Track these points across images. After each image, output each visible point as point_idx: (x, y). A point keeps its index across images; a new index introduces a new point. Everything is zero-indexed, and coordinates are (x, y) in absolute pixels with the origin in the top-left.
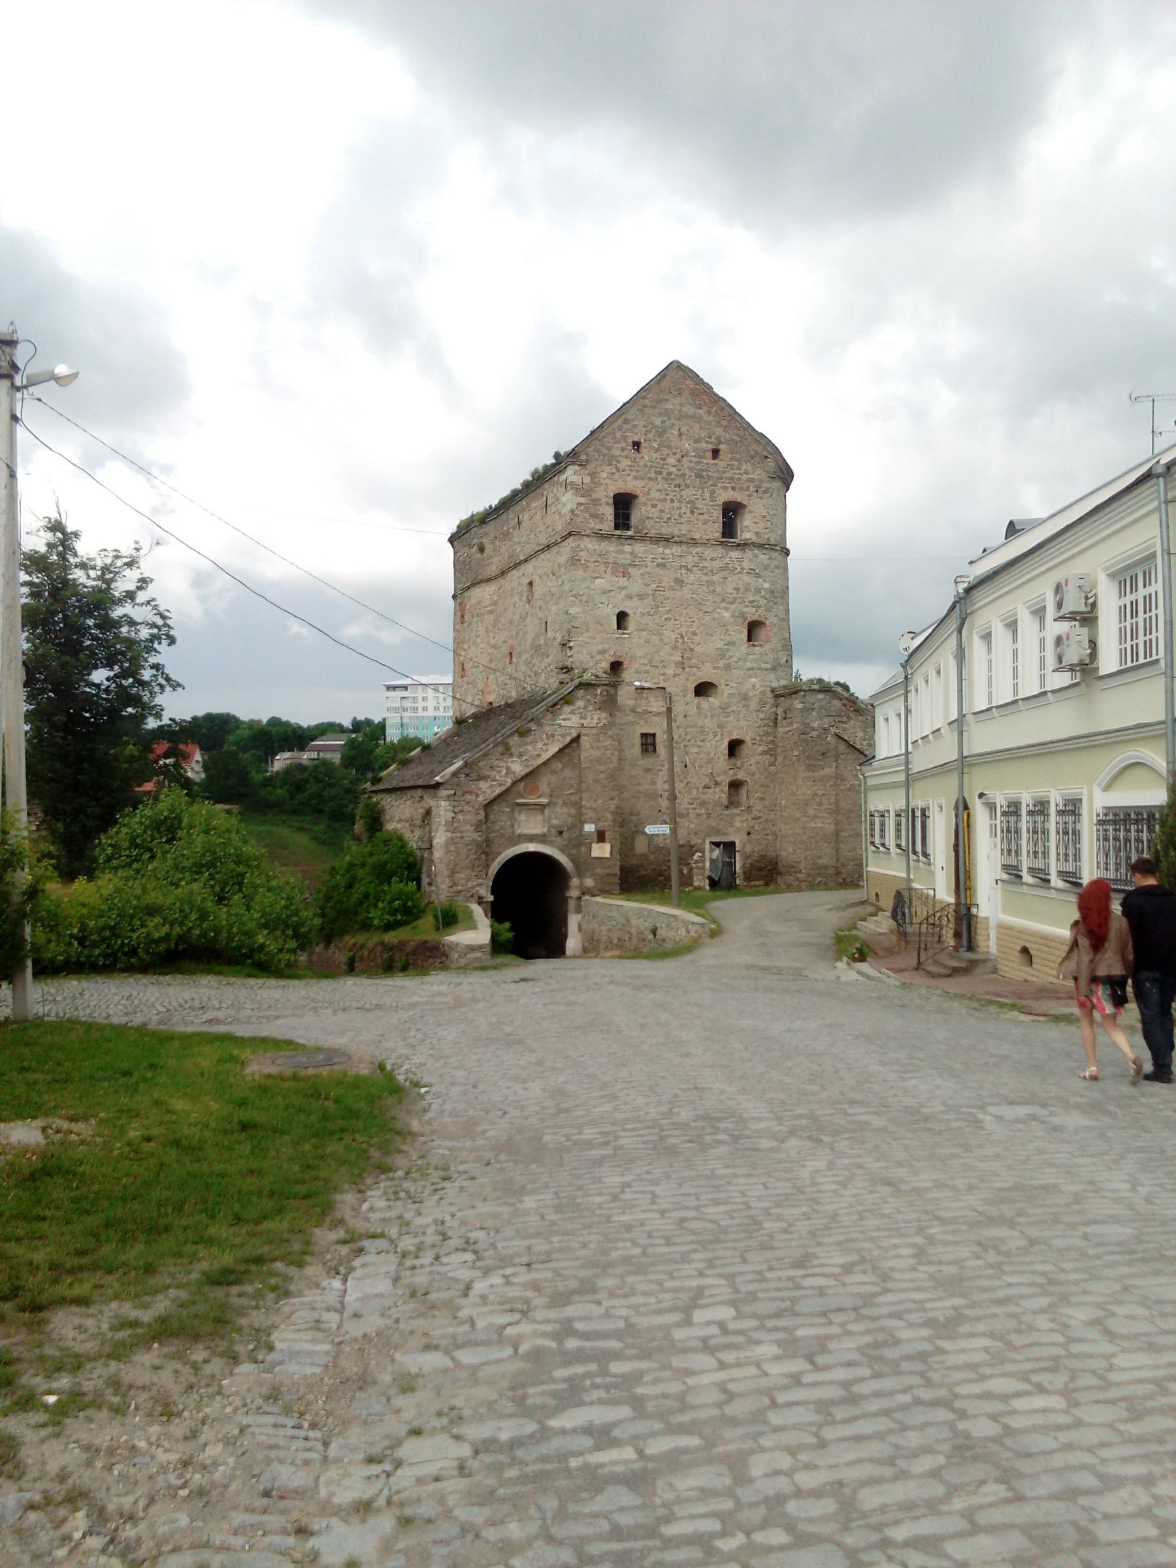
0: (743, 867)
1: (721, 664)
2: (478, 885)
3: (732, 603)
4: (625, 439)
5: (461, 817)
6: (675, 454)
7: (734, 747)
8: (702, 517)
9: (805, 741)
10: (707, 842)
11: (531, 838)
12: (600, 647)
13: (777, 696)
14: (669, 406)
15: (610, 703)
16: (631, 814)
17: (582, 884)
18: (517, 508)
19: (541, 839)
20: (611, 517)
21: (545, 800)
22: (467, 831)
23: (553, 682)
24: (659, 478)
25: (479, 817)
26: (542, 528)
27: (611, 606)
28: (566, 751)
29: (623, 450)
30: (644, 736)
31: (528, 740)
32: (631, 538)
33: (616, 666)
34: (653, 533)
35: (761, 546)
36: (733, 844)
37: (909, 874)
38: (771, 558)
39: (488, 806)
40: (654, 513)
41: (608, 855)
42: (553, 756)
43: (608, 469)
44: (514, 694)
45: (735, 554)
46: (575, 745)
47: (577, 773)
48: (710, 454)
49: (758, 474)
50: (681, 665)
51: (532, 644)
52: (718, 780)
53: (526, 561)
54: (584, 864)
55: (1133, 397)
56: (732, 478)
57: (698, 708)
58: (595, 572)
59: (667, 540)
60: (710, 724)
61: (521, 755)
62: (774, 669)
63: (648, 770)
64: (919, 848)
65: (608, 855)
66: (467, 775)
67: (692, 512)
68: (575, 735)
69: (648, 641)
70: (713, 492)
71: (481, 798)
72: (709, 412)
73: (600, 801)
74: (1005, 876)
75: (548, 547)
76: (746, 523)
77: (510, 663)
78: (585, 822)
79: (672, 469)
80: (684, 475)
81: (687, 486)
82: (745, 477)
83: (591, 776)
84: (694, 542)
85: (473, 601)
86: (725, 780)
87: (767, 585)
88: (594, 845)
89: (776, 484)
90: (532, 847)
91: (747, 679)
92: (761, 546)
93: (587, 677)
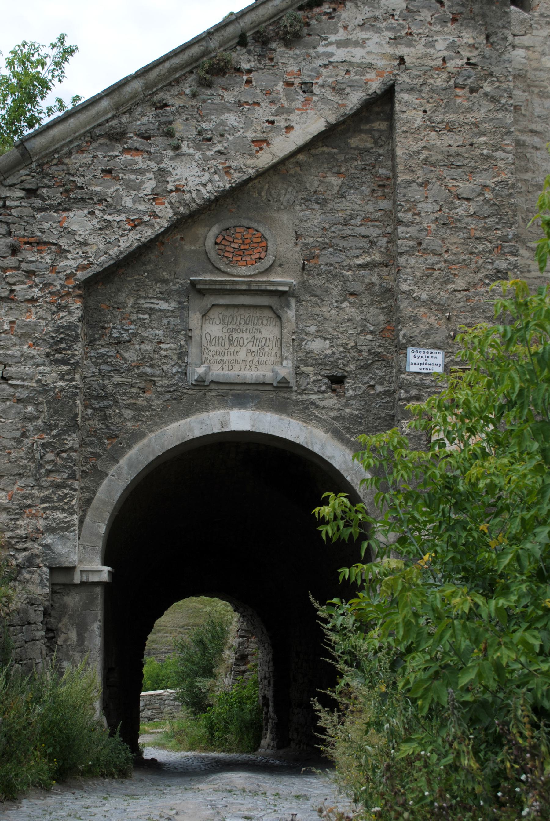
2: (49, 530)
21: (282, 279)
22: (27, 358)
25: (64, 318)
28: (354, 142)
31: (229, 97)
46: (380, 125)
47: (386, 204)
66: (31, 193)
68: (376, 85)
71: (69, 263)
78: (411, 341)
90: (241, 420)
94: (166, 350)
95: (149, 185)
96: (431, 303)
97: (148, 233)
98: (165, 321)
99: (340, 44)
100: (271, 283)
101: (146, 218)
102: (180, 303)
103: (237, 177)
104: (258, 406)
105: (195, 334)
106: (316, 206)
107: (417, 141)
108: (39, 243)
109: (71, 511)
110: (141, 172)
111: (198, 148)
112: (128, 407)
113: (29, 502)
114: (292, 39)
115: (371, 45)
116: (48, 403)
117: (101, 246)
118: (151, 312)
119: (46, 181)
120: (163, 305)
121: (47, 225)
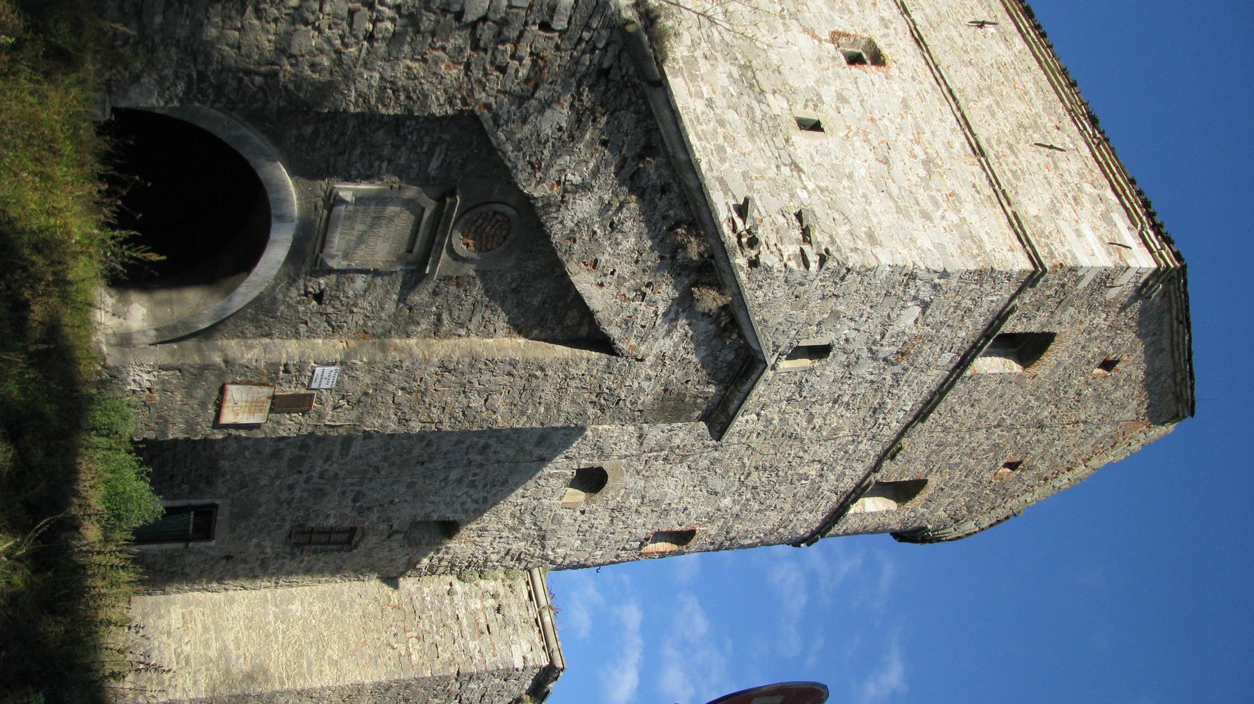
10: (218, 502)
27: (853, 334)
41: (228, 417)
43: (1104, 325)
59: (921, 415)
65: (228, 417)
68: (622, 346)
75: (978, 151)
88: (267, 391)
94: (380, 166)
96: (386, 379)
98: (415, 165)
100: (436, 262)
101: (538, 175)
102: (434, 179)
106: (513, 286)
112: (316, 134)
113: (200, 60)
117: (519, 136)
118: (430, 154)
119: (613, 90)
120: (434, 164)
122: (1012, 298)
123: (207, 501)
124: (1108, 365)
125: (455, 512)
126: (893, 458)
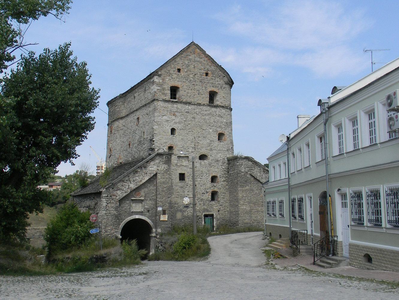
0: (216, 224)
1: (209, 148)
2: (115, 232)
3: (212, 126)
4: (175, 68)
5: (109, 205)
6: (193, 73)
7: (214, 179)
8: (202, 96)
9: (240, 176)
11: (137, 213)
12: (165, 141)
13: (228, 160)
14: (190, 57)
15: (168, 162)
16: (175, 204)
17: (156, 231)
18: (134, 92)
19: (141, 213)
20: (170, 95)
21: (142, 198)
23: (146, 154)
24: (187, 81)
25: (117, 205)
26: (143, 98)
29: (174, 71)
30: (179, 173)
31: (137, 175)
32: (176, 102)
33: (171, 148)
34: (184, 100)
35: (223, 107)
36: (212, 216)
37: (290, 226)
38: (226, 111)
39: (121, 201)
40: (185, 93)
41: (167, 220)
42: (147, 181)
43: (168, 77)
44: (130, 159)
45: (214, 109)
46: (155, 177)
48: (205, 74)
49: (221, 82)
50: (195, 148)
51: (138, 140)
52: (208, 191)
53: (137, 110)
54: (158, 222)
55: (365, 50)
56: (213, 83)
57: (201, 164)
58: (163, 113)
59: (190, 103)
60: (204, 170)
61: (134, 181)
62: (227, 150)
63: (182, 187)
64: (297, 214)
67: (199, 94)
68: (155, 173)
69: (182, 139)
70: (206, 87)
71: (117, 198)
72: (205, 60)
73: (164, 199)
74: (353, 223)
75: (146, 105)
76: (217, 99)
77: (130, 147)
79: (191, 79)
80: (195, 81)
81: (197, 85)
82: (217, 83)
83: (160, 189)
84: (199, 104)
85: (116, 125)
86: (210, 191)
87: (225, 121)
89: (227, 86)
90: (137, 217)
91: (218, 154)
92: (223, 107)
93: (161, 151)
95: (128, 187)
97: (127, 193)
99: (151, 167)
103: (138, 186)
104: (139, 215)
105: (132, 206)
107: (160, 180)
108: (114, 195)
109: (118, 230)
110: (126, 185)
111: (133, 182)
114: (145, 167)
115: (154, 168)
116: (115, 216)
118: (126, 203)
121: (115, 193)
122: (161, 101)
123: (203, 216)
124: (179, 70)
125: (209, 177)
126: (200, 104)
